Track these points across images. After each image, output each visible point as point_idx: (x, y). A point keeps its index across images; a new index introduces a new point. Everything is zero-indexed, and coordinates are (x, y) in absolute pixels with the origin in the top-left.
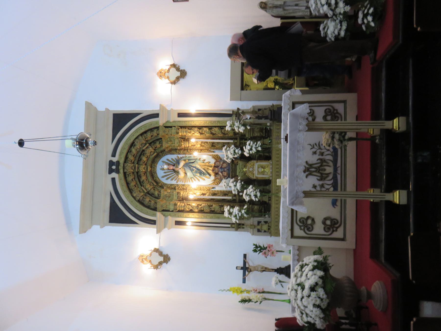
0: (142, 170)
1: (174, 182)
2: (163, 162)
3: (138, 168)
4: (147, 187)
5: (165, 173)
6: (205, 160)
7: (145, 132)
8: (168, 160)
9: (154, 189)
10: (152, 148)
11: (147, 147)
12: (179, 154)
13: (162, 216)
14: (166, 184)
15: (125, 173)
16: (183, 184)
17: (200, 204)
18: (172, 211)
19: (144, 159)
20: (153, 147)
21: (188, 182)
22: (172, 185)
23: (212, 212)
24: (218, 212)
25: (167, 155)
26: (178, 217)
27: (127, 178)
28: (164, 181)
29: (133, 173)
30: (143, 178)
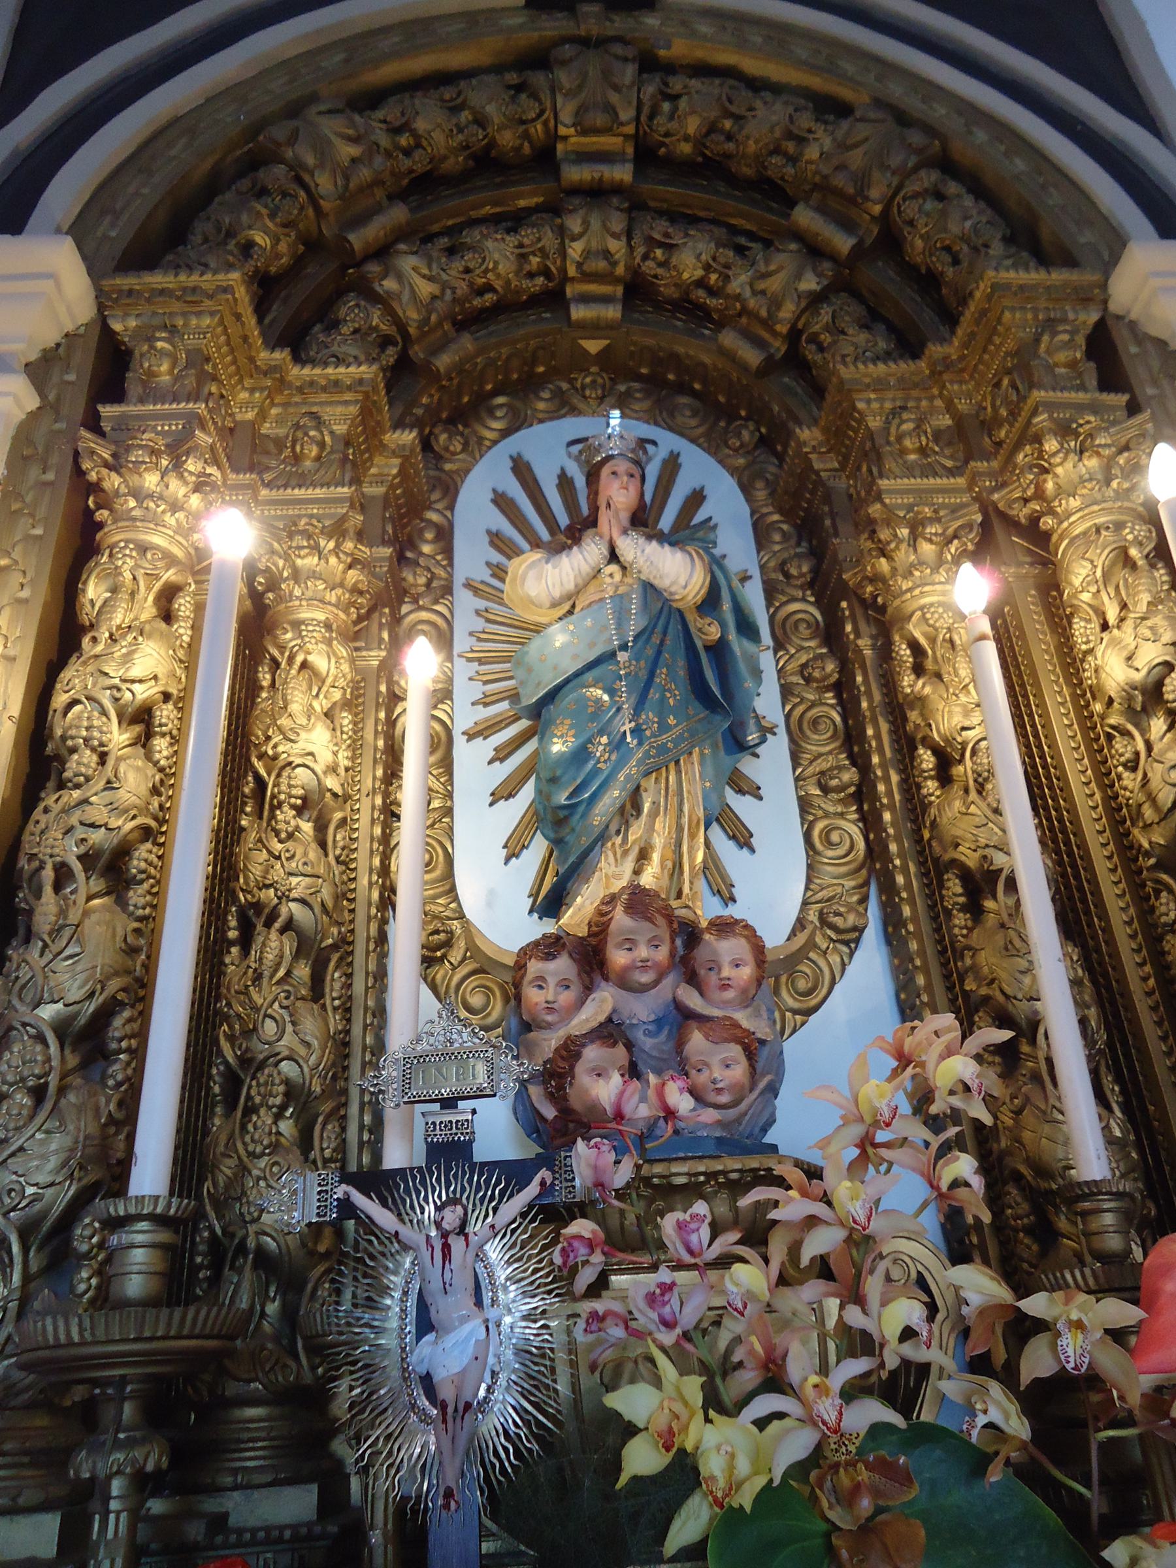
0: (574, 224)
1: (471, 557)
2: (672, 466)
3: (597, 193)
4: (408, 263)
7: (979, 188)
8: (697, 498)
9: (385, 342)
10: (816, 300)
11: (814, 251)
12: (770, 592)
13: (50, 336)
14: (450, 490)
15: (538, 59)
16: (462, 642)
17: (161, 745)
18: (93, 424)
19: (691, 259)
20: (825, 314)
22: (445, 536)
27: (490, 79)
29: (544, 159)
30: (499, 258)
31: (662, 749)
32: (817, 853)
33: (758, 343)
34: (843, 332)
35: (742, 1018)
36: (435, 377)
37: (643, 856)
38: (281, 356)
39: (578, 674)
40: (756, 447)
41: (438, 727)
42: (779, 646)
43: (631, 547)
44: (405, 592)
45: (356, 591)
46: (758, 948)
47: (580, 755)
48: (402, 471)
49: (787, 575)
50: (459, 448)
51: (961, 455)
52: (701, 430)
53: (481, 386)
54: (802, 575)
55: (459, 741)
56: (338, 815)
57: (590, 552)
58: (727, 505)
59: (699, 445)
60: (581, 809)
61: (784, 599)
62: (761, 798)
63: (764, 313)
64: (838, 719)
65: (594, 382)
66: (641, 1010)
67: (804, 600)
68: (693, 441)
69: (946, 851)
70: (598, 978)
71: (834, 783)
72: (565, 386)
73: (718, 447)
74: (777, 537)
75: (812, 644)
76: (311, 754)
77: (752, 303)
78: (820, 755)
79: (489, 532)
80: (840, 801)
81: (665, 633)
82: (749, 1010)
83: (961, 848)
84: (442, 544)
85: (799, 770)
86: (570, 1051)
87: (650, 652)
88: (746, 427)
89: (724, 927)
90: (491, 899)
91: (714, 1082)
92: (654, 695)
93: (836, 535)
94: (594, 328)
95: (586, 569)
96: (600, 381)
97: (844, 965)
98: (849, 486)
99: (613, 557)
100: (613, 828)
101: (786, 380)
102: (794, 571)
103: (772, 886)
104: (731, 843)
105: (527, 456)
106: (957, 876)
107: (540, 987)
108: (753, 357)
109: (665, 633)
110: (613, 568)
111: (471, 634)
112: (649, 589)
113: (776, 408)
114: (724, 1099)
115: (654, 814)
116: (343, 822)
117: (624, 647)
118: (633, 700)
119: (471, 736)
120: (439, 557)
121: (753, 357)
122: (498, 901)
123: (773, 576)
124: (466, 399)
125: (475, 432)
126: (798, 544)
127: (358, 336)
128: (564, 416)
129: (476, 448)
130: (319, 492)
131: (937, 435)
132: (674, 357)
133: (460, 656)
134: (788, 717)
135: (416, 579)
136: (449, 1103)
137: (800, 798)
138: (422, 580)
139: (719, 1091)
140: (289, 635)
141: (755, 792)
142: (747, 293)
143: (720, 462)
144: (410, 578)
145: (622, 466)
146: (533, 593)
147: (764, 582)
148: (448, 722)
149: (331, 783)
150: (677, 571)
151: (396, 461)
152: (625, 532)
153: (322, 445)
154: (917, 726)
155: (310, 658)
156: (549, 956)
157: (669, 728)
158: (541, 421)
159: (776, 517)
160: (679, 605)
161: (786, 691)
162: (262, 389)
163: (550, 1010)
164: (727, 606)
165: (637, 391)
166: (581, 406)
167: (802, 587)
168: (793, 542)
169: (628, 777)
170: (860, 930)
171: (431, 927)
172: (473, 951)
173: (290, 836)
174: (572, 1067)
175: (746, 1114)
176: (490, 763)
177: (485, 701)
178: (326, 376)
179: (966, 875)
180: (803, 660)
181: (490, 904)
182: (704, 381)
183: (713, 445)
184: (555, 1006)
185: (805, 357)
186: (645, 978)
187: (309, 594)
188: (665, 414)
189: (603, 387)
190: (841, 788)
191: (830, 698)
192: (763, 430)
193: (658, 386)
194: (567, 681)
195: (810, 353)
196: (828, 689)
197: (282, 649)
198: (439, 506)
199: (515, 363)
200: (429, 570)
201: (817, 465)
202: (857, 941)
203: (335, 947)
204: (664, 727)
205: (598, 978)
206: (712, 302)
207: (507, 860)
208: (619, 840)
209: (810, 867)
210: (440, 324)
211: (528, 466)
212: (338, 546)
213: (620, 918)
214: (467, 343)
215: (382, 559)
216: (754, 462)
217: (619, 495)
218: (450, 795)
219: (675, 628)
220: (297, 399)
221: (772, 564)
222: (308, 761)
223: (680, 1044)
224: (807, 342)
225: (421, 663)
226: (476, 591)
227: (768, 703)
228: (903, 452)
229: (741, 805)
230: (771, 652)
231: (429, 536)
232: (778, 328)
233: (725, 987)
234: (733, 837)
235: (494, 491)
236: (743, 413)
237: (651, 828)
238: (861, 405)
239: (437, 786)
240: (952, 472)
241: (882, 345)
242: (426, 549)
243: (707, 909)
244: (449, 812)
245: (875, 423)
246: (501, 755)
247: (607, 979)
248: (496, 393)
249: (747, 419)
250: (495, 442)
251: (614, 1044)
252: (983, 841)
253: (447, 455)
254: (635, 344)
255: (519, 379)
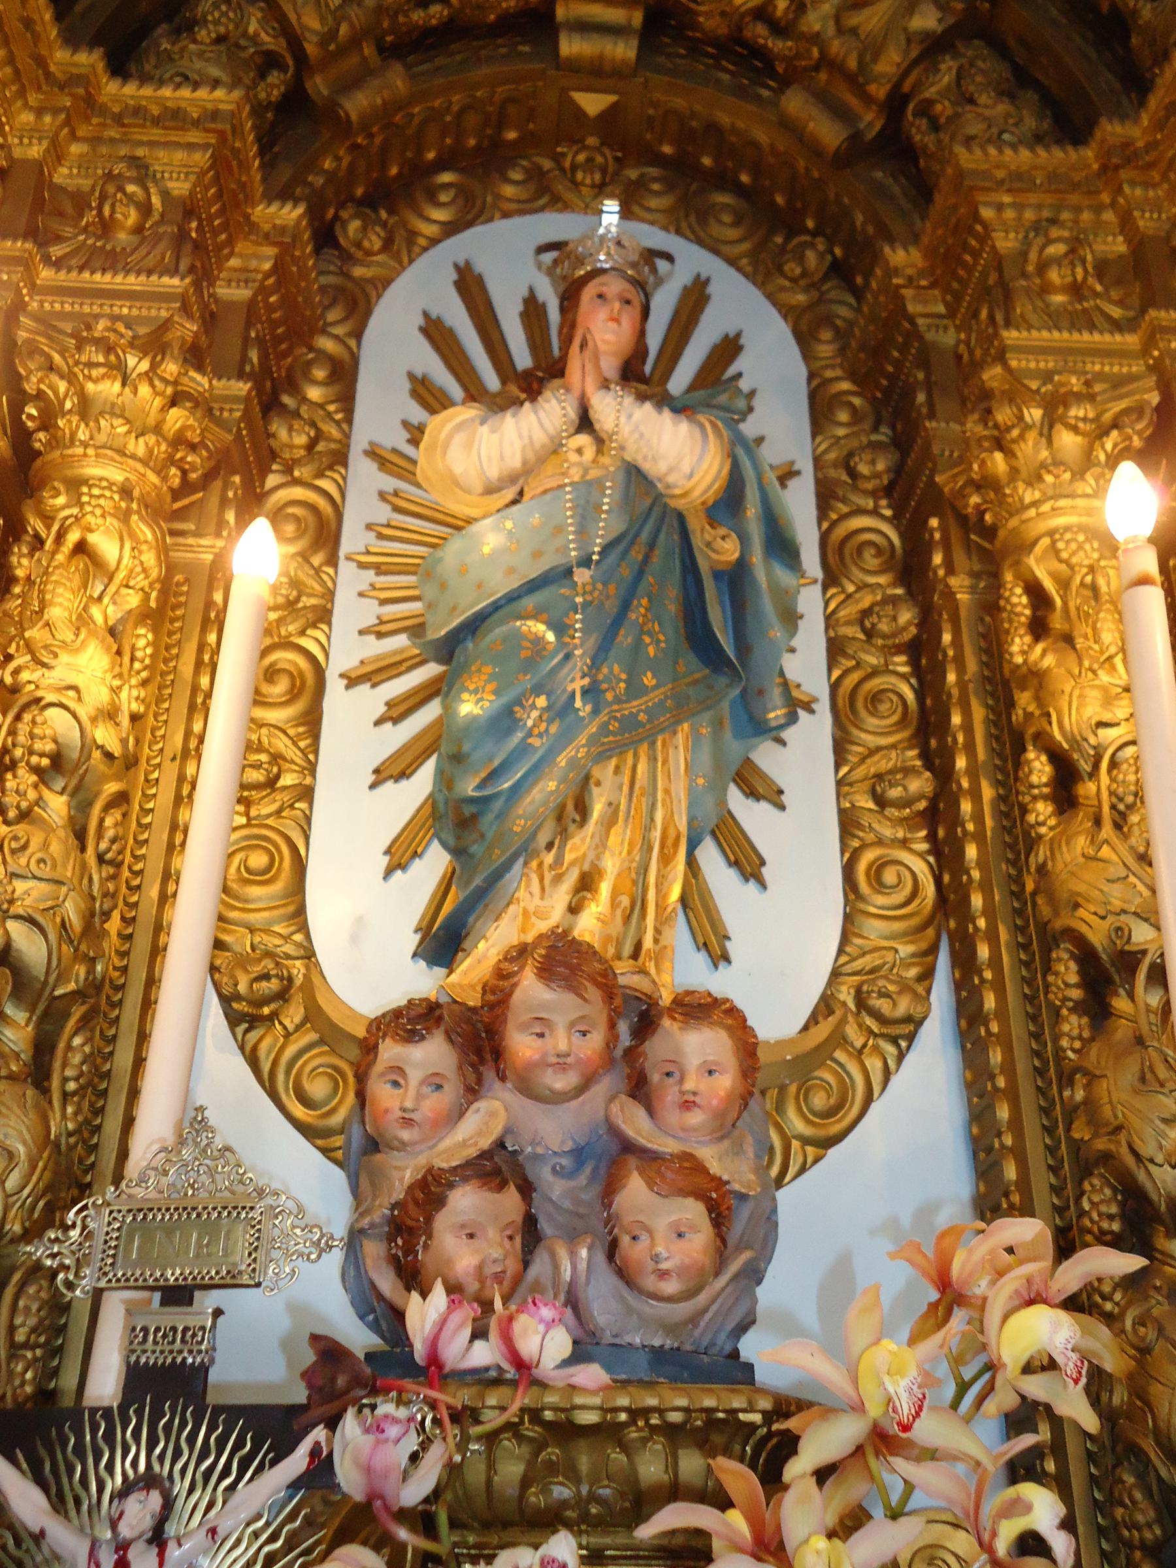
1: (380, 410)
8: (729, 348)
9: (269, 62)
10: (934, 47)
12: (826, 496)
14: (359, 305)
16: (353, 539)
22: (344, 376)
31: (630, 724)
32: (860, 897)
33: (840, 113)
34: (972, 101)
35: (712, 1158)
36: (344, 128)
37: (586, 884)
38: (88, 60)
39: (512, 597)
40: (825, 278)
41: (302, 663)
42: (831, 579)
43: (615, 410)
44: (274, 455)
45: (179, 440)
46: (747, 1045)
47: (504, 721)
48: (278, 268)
49: (853, 474)
50: (377, 244)
51: (1135, 300)
52: (746, 246)
53: (420, 152)
54: (877, 475)
55: (334, 687)
56: (112, 787)
57: (550, 414)
58: (774, 366)
59: (739, 270)
60: (497, 805)
61: (845, 509)
62: (782, 808)
63: (852, 64)
64: (910, 695)
65: (590, 160)
66: (551, 1131)
67: (875, 512)
68: (732, 262)
69: (1056, 913)
70: (489, 1075)
71: (895, 793)
72: (547, 164)
73: (768, 274)
74: (843, 416)
75: (882, 580)
76: (75, 688)
77: (836, 47)
78: (879, 749)
79: (411, 376)
80: (902, 821)
81: (652, 545)
82: (726, 1143)
83: (1081, 912)
84: (336, 388)
85: (844, 770)
86: (430, 1192)
87: (626, 572)
88: (812, 245)
89: (700, 1008)
90: (358, 932)
91: (656, 1258)
92: (625, 638)
93: (932, 415)
94: (595, 74)
95: (540, 438)
96: (599, 159)
97: (887, 1075)
98: (959, 341)
99: (585, 423)
100: (543, 838)
101: (879, 175)
102: (863, 469)
103: (784, 941)
104: (732, 874)
105: (479, 267)
106: (1073, 956)
107: (396, 1084)
108: (829, 133)
109: (652, 545)
110: (583, 439)
111: (369, 527)
112: (635, 476)
113: (859, 219)
114: (670, 1287)
115: (610, 821)
116: (122, 798)
117: (586, 562)
118: (592, 642)
119: (351, 681)
120: (331, 408)
121: (829, 133)
122: (365, 934)
123: (832, 473)
124: (394, 171)
125: (404, 224)
126: (875, 429)
127: (222, 48)
128: (542, 209)
129: (403, 247)
130: (133, 282)
131: (1102, 268)
132: (712, 127)
133: (348, 558)
134: (834, 688)
135: (290, 437)
136: (178, 1295)
137: (842, 812)
138: (301, 440)
139: (664, 1275)
140: (61, 500)
141: (775, 797)
142: (831, 30)
143: (770, 297)
144: (283, 434)
145: (614, 286)
146: (458, 469)
147: (818, 482)
148: (321, 657)
149: (104, 735)
150: (678, 452)
151: (272, 251)
152: (605, 385)
153: (145, 209)
154: (1028, 716)
155: (92, 538)
156: (412, 1037)
157: (645, 690)
158: (506, 215)
159: (845, 386)
160: (679, 504)
161: (835, 649)
162: (56, 111)
163: (408, 1122)
164: (752, 510)
165: (655, 180)
166: (569, 196)
167: (873, 494)
168: (867, 426)
169: (573, 763)
170: (915, 1022)
171: (257, 969)
172: (314, 1016)
173: (25, 815)
174: (429, 1220)
175: (705, 1310)
176: (378, 723)
178: (159, 101)
179: (1086, 956)
180: (867, 601)
181: (355, 939)
182: (756, 170)
183: (762, 270)
184: (415, 1116)
185: (909, 138)
186: (561, 1082)
187: (102, 438)
188: (692, 219)
189: (604, 170)
190: (907, 802)
191: (901, 664)
192: (838, 251)
193: (686, 174)
194: (496, 607)
195: (919, 133)
196: (899, 649)
197: (48, 520)
198: (339, 330)
199: (471, 120)
200: (313, 424)
201: (911, 308)
202: (911, 1038)
203: (78, 995)
204: (635, 689)
205: (489, 1075)
206: (778, 45)
207: (388, 873)
208: (549, 858)
209: (848, 918)
210: (355, 42)
211: (480, 280)
212: (154, 366)
213: (530, 988)
214: (397, 80)
215: (234, 399)
216: (820, 301)
217: (606, 331)
218: (312, 768)
219: (668, 539)
220: (113, 133)
221: (832, 456)
222: (69, 698)
223: (610, 1190)
224: (915, 115)
225: (258, 558)
227: (806, 663)
228: (1046, 289)
229: (752, 816)
230: (818, 588)
231: (320, 374)
232: (873, 88)
233: (687, 1105)
234: (735, 864)
235: (426, 314)
236: (810, 224)
237: (601, 845)
238: (987, 213)
239: (292, 753)
240: (1117, 326)
241: (1030, 122)
242: (314, 393)
243: (685, 970)
244: (307, 793)
245: (1005, 243)
246: (396, 712)
247: (503, 1079)
248: (441, 165)
249: (814, 234)
250: (434, 242)
251: (501, 1187)
252: (1117, 904)
253: (359, 254)
254: (655, 105)
255: (477, 148)
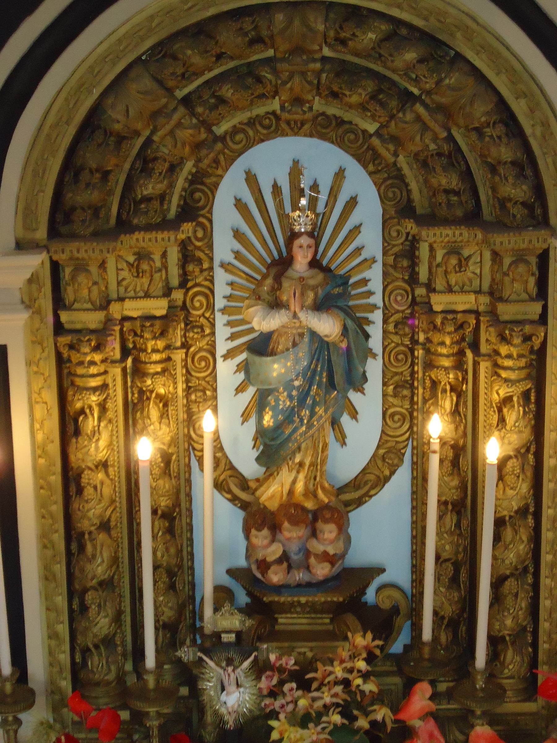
2: (340, 175)
5: (276, 189)
6: (354, 414)
8: (352, 202)
12: (385, 274)
16: (220, 302)
21: (228, 331)
22: (208, 237)
23: (75, 540)
24: (77, 573)
25: (383, 199)
26: (29, 363)
28: (230, 187)
55: (219, 360)
119: (225, 357)
177: (232, 337)
207: (242, 423)
226: (227, 270)
227: (376, 342)
